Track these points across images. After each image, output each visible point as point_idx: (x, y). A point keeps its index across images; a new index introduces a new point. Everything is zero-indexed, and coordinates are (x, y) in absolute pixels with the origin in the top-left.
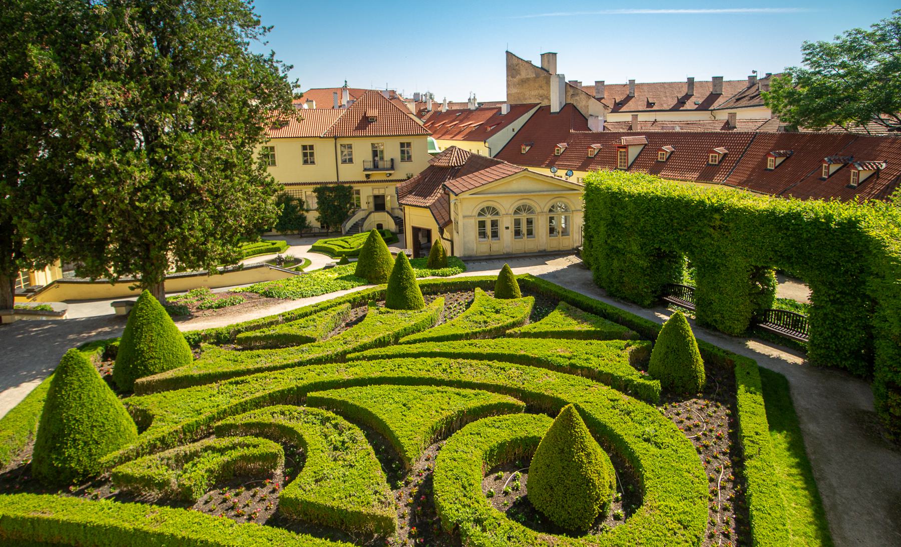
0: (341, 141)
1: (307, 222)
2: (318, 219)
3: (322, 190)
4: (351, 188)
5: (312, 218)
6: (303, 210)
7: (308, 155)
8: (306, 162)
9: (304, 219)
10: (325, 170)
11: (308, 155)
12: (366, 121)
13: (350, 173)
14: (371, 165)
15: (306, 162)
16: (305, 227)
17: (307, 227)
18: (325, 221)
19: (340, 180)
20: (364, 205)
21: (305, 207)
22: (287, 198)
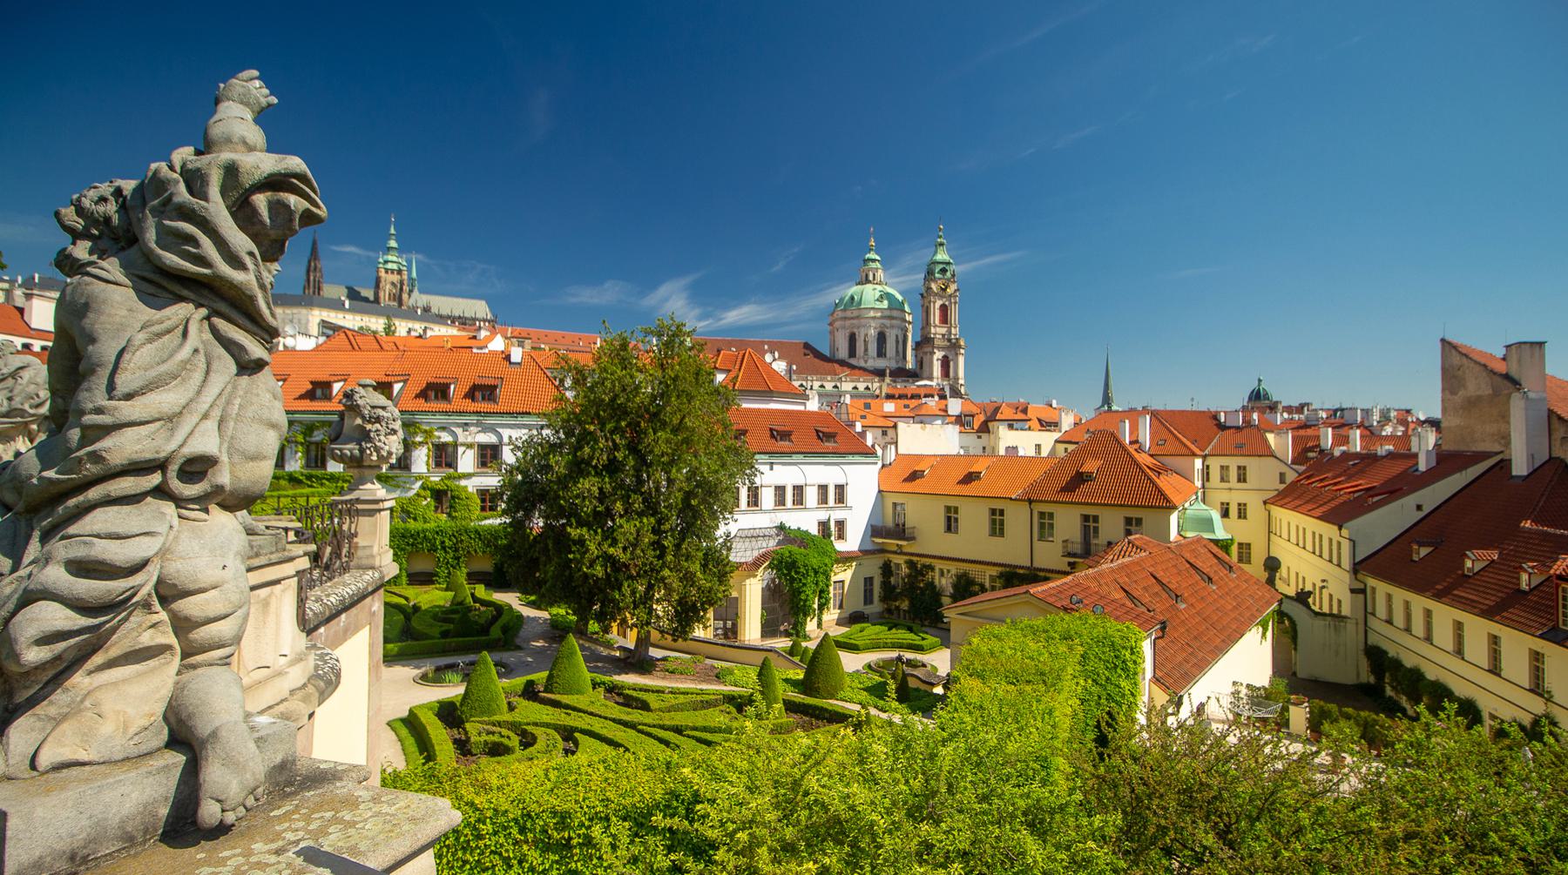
0: (1038, 508)
8: (993, 533)
11: (997, 526)
12: (1080, 479)
14: (1078, 549)
15: (993, 533)
19: (1036, 565)
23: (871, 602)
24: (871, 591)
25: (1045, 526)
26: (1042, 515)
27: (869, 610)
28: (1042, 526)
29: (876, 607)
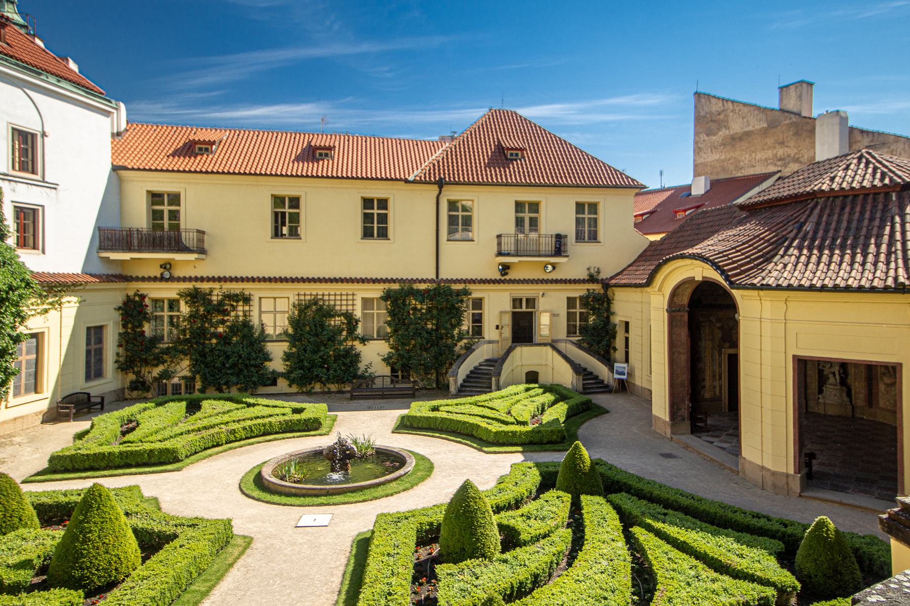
1: (362, 366)
2: (387, 360)
3: (398, 297)
4: (466, 293)
5: (374, 355)
6: (356, 338)
7: (375, 222)
8: (367, 234)
9: (353, 358)
10: (411, 252)
11: (375, 222)
13: (467, 260)
15: (367, 234)
16: (355, 376)
17: (362, 377)
18: (400, 365)
19: (443, 276)
20: (489, 332)
21: (359, 331)
22: (321, 308)
23: (99, 374)
24: (99, 352)
25: (459, 221)
26: (452, 205)
27: (96, 388)
28: (452, 221)
29: (111, 379)
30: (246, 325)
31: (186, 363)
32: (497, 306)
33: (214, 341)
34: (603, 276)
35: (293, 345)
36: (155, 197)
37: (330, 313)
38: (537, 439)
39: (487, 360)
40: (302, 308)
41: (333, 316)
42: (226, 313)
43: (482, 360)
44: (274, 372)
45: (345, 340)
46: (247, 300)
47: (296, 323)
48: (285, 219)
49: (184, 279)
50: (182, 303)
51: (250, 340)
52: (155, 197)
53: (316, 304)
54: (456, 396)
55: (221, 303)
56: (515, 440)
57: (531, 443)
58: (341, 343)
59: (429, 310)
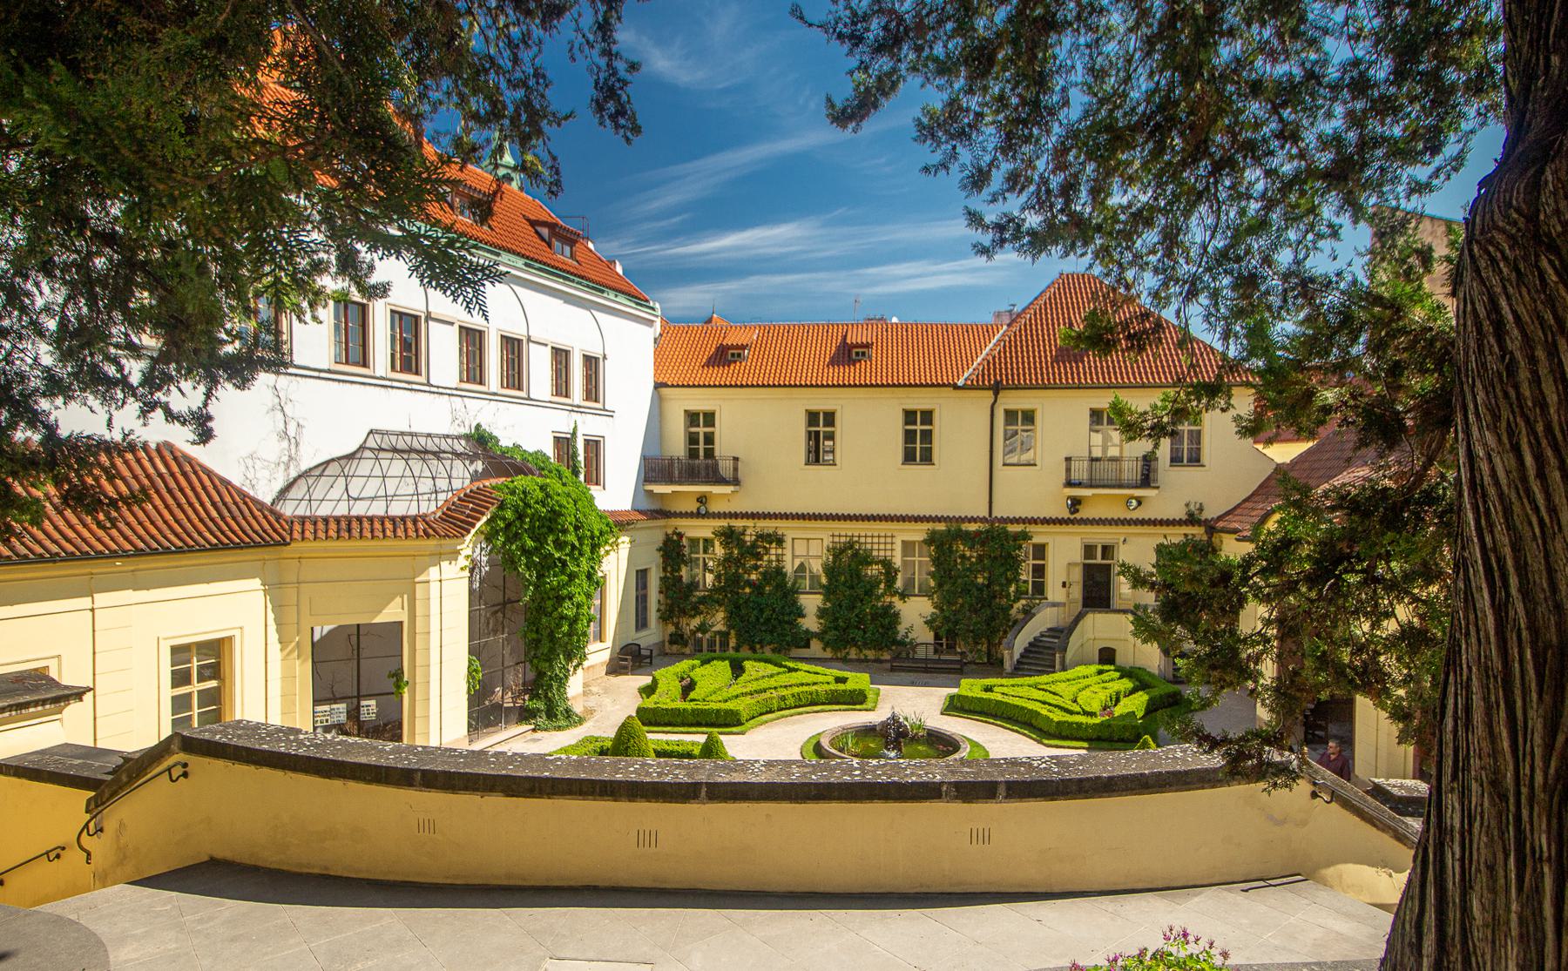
1: (902, 629)
3: (946, 540)
4: (1026, 536)
5: (915, 615)
7: (918, 444)
9: (889, 618)
11: (918, 444)
13: (1030, 492)
16: (895, 642)
17: (902, 643)
18: (946, 630)
19: (997, 513)
20: (1054, 592)
21: (899, 584)
22: (856, 554)
30: (779, 572)
31: (720, 615)
32: (1063, 555)
33: (747, 590)
34: (1209, 514)
35: (827, 599)
36: (692, 417)
37: (866, 559)
38: (1106, 734)
39: (1050, 630)
40: (837, 552)
41: (870, 564)
42: (759, 557)
43: (1044, 629)
44: (807, 631)
45: (883, 595)
46: (780, 541)
47: (830, 571)
48: (819, 438)
49: (719, 516)
50: (717, 543)
51: (781, 590)
52: (692, 417)
53: (851, 547)
54: (1012, 675)
55: (754, 545)
56: (1081, 734)
57: (1099, 739)
58: (878, 598)
59: (980, 558)
